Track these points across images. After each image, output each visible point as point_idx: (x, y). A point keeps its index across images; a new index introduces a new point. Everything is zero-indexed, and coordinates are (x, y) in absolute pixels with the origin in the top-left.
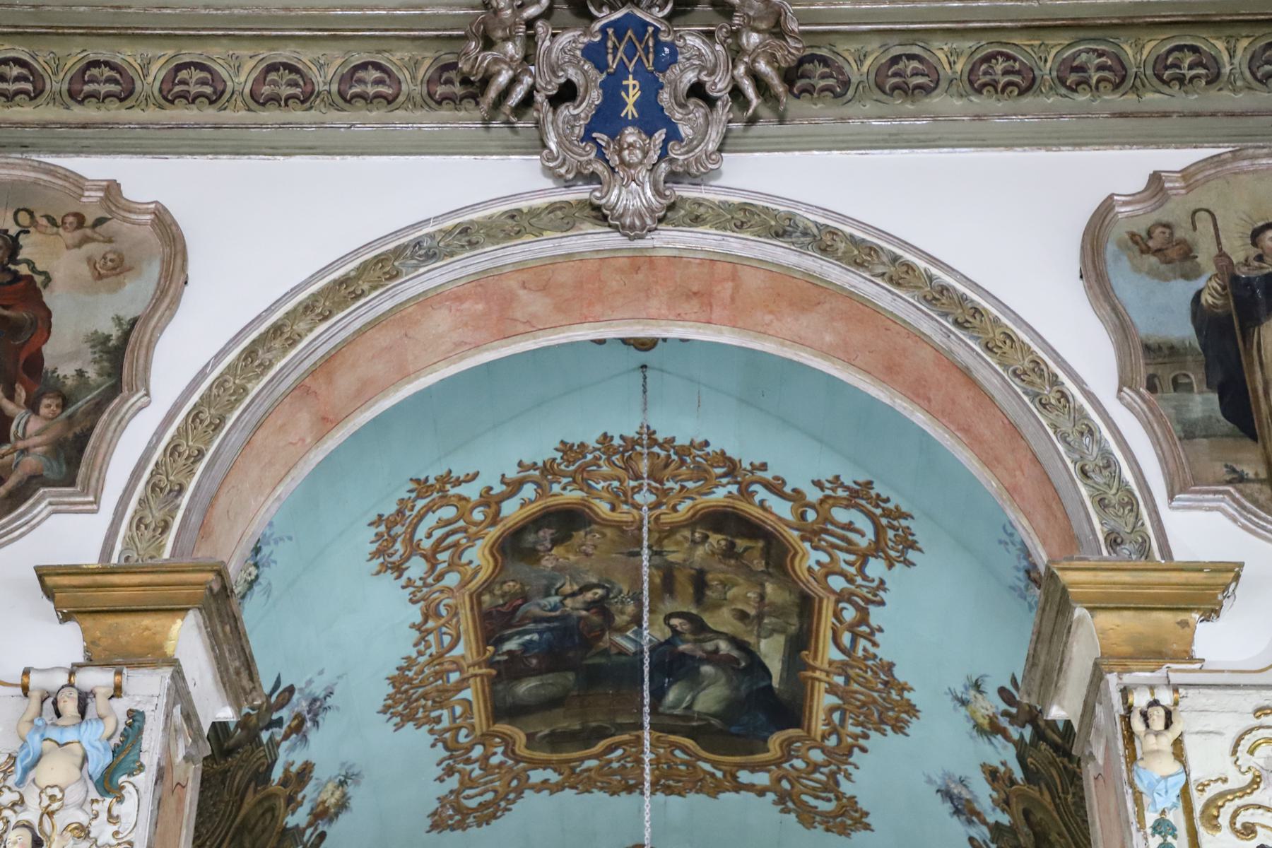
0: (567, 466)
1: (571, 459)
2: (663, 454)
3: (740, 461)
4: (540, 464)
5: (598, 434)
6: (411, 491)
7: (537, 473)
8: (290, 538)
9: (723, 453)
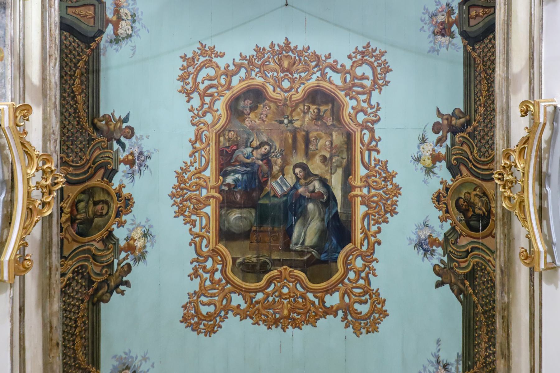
1: (260, 57)
2: (293, 56)
4: (248, 58)
5: (269, 44)
7: (246, 62)
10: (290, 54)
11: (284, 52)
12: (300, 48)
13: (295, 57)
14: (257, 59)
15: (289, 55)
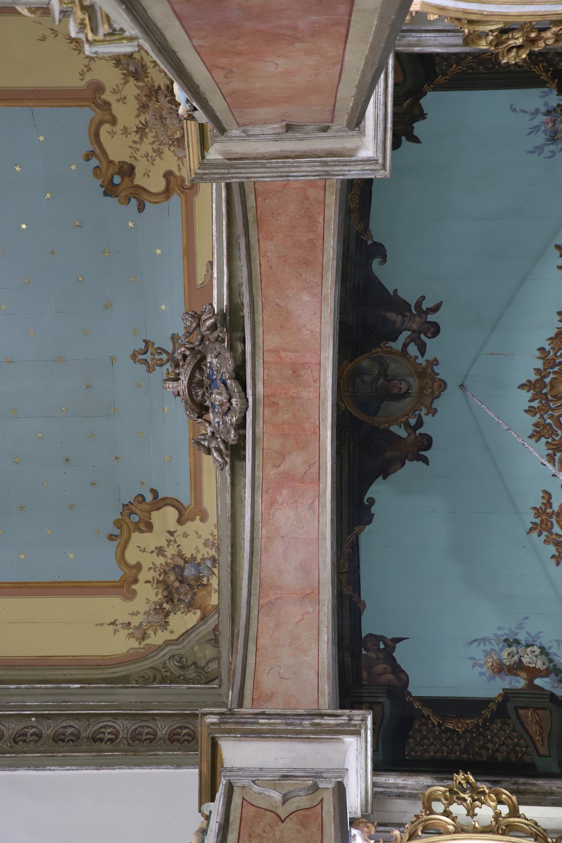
0: (557, 435)
1: (551, 432)
2: (552, 376)
3: (558, 328)
4: (550, 452)
6: (540, 535)
7: (558, 454)
8: (526, 618)
9: (551, 339)
10: (547, 380)
11: (545, 391)
12: (539, 364)
13: (554, 372)
14: (554, 437)
15: (551, 383)
